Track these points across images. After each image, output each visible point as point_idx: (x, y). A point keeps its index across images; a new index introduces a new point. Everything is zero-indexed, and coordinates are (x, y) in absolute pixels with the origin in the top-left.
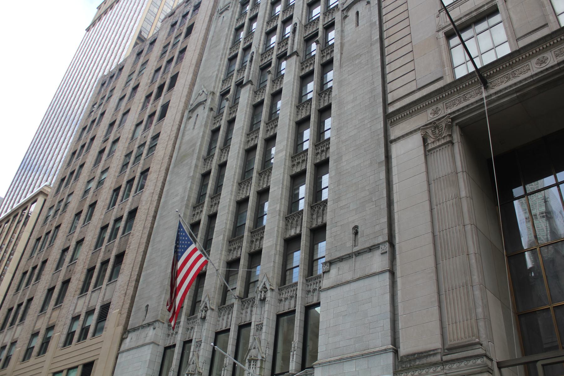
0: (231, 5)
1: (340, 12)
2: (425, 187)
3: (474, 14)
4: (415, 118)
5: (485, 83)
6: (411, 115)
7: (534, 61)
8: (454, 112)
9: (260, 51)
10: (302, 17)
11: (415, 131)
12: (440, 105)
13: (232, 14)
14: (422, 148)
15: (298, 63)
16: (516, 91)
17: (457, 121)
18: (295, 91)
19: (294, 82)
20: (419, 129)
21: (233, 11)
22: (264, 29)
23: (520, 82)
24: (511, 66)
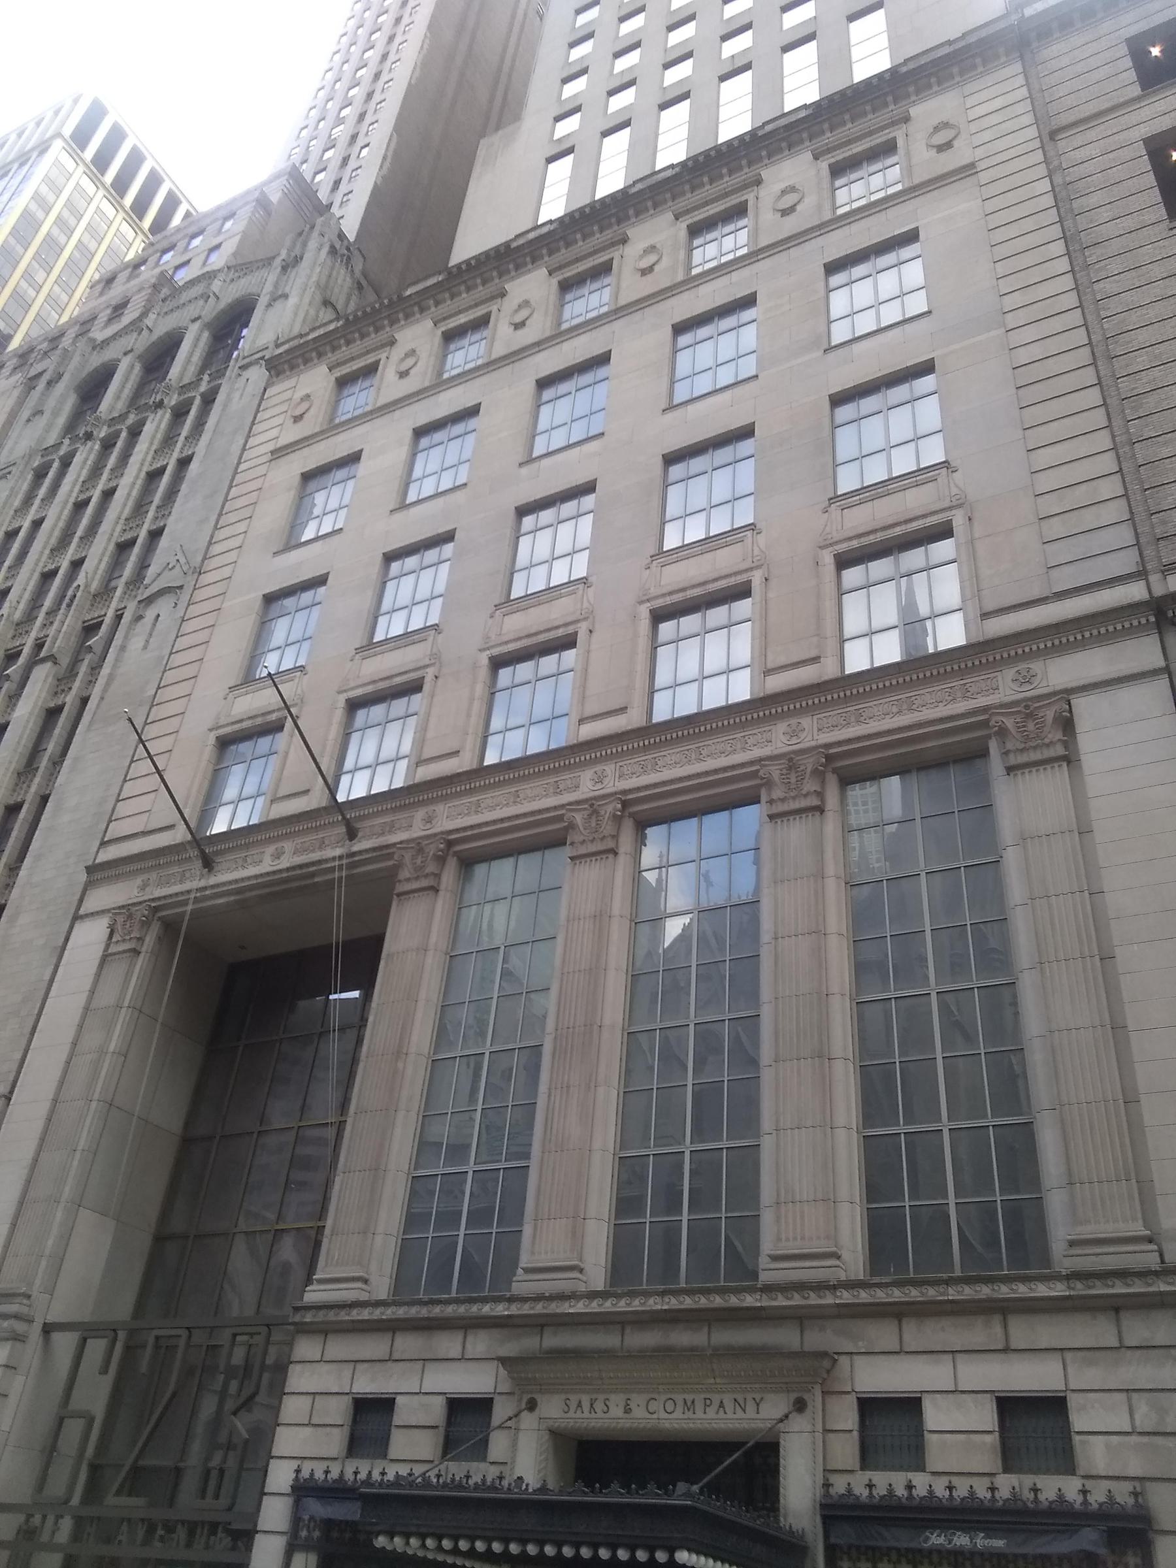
0: (13, 469)
1: (136, 602)
2: (77, 1019)
3: (259, 721)
4: (120, 885)
5: (208, 864)
6: (118, 878)
7: (270, 849)
8: (159, 899)
9: (17, 615)
10: (95, 573)
11: (103, 912)
12: (153, 876)
13: (9, 497)
14: (103, 946)
15: (50, 679)
16: (239, 891)
17: (164, 913)
18: (23, 742)
19: (28, 721)
20: (108, 911)
21: (12, 489)
22: (41, 564)
23: (236, 881)
24: (247, 846)
